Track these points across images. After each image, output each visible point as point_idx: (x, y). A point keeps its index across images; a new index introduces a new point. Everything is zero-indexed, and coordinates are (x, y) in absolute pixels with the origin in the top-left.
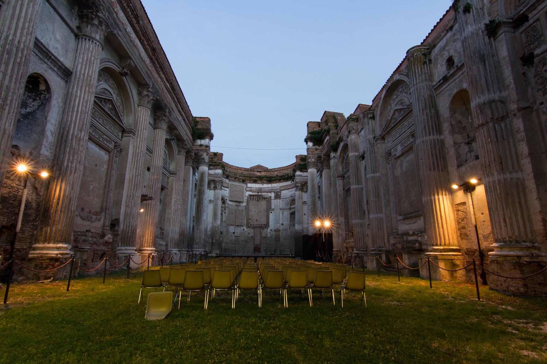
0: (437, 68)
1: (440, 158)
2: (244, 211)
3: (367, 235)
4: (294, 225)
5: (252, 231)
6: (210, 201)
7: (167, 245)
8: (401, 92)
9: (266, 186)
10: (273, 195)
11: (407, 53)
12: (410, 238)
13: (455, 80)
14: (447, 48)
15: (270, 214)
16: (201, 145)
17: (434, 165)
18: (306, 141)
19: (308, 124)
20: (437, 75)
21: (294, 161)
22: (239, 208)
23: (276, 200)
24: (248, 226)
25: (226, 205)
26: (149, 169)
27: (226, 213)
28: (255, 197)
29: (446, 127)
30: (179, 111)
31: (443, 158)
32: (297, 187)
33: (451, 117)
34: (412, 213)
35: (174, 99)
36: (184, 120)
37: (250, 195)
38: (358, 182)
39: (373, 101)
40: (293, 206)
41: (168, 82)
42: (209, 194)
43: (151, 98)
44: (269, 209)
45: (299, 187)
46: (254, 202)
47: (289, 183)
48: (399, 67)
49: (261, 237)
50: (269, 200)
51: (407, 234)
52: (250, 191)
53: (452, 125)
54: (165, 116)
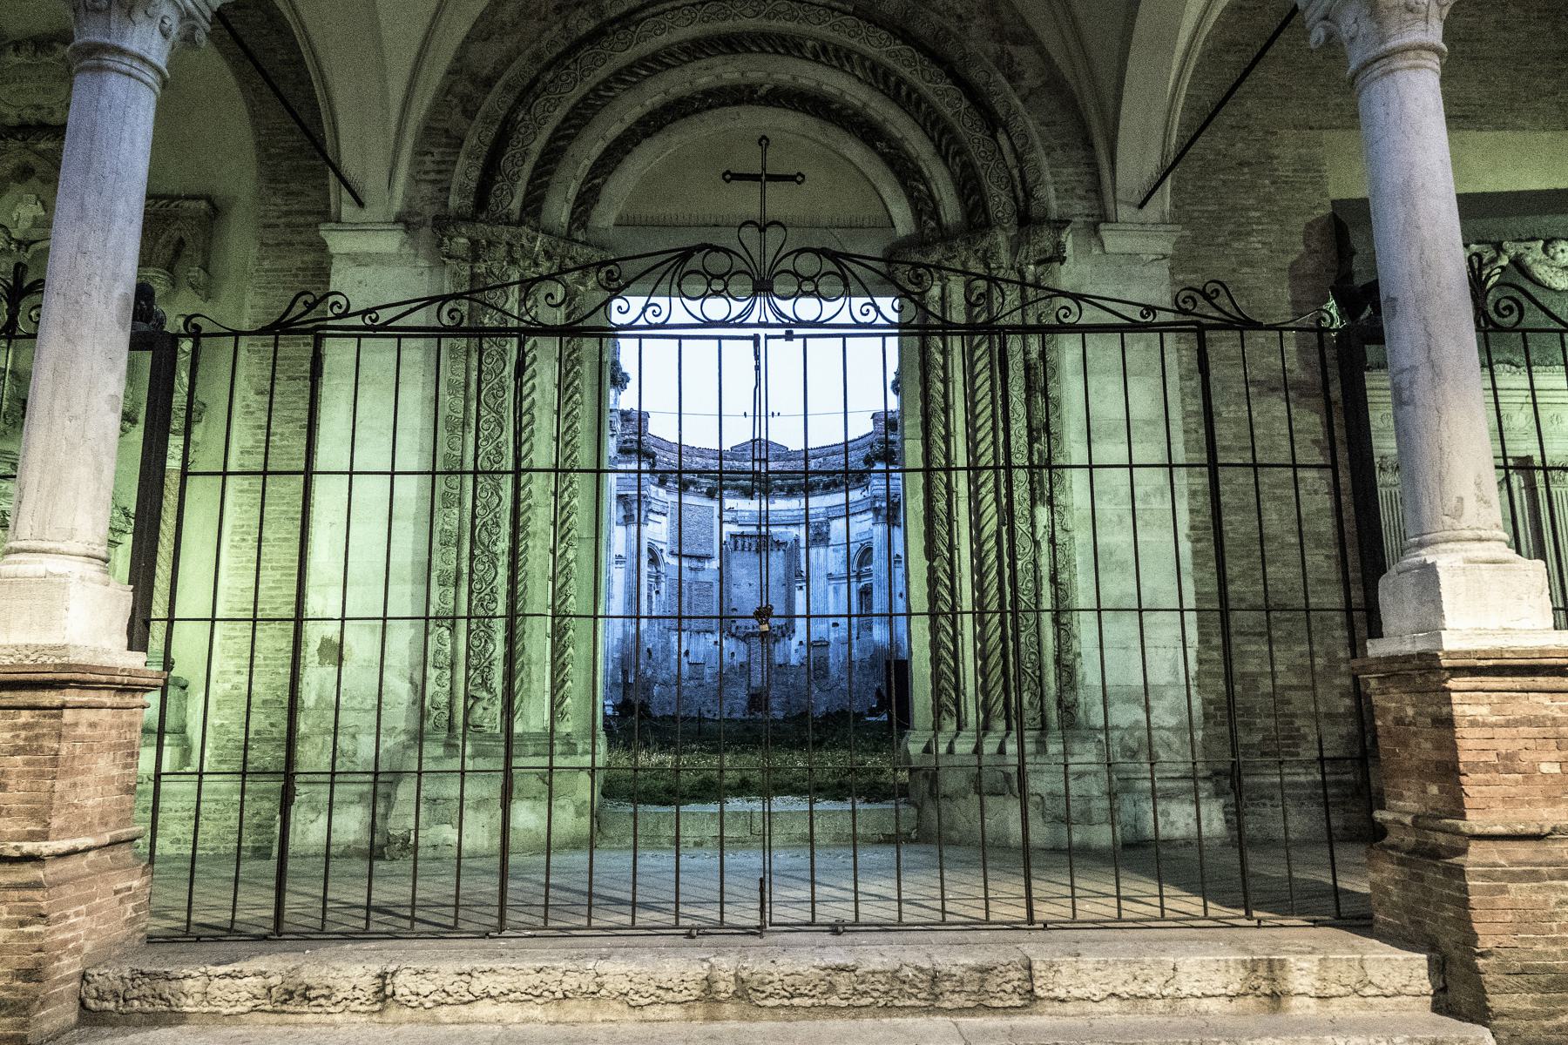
4: (871, 629)
5: (742, 644)
22: (702, 577)
25: (662, 569)
27: (663, 592)
32: (877, 511)
37: (733, 536)
45: (884, 512)
49: (770, 666)
50: (791, 550)
52: (734, 521)
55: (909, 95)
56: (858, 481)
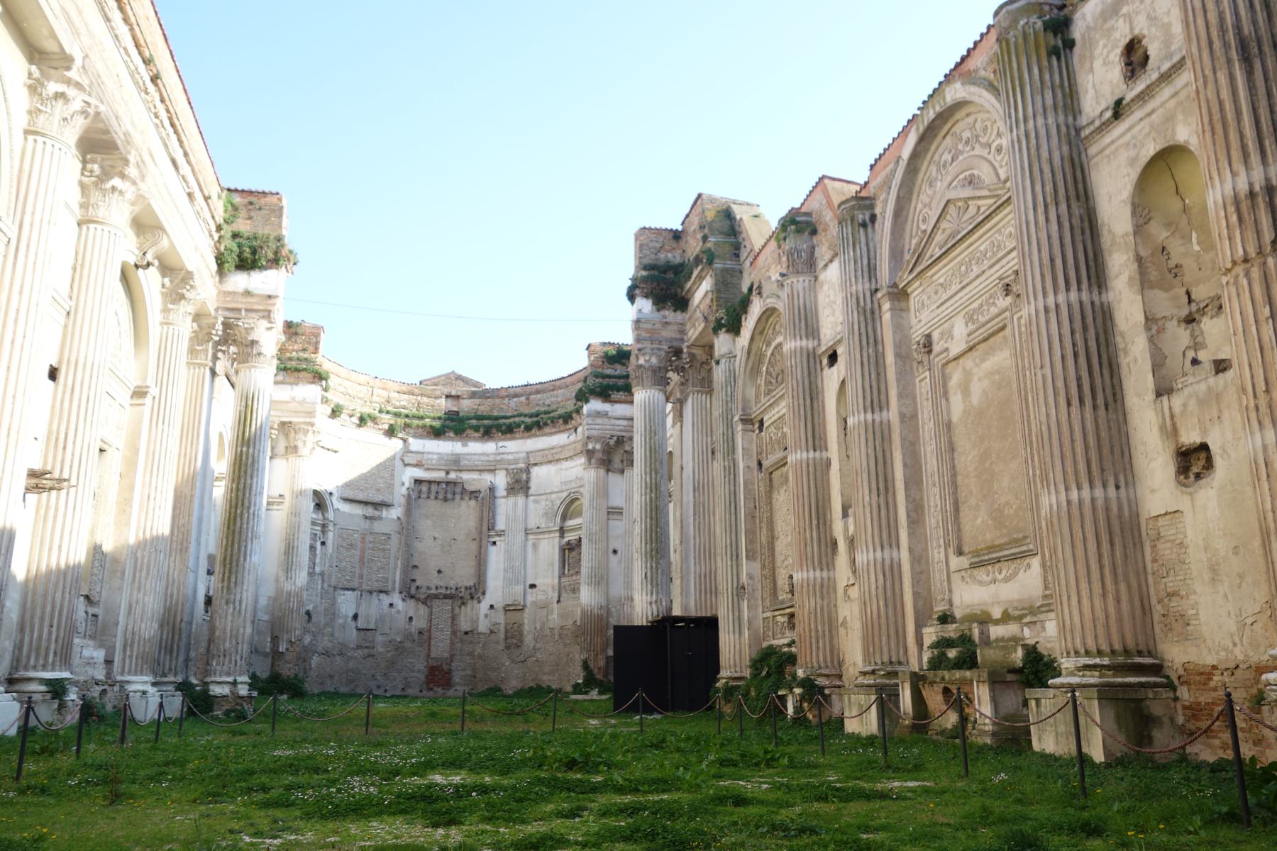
0: (1091, 70)
1: (1101, 364)
2: (395, 540)
3: (844, 623)
4: (575, 590)
5: (423, 610)
7: (109, 662)
8: (967, 143)
9: (477, 448)
10: (501, 480)
11: (996, 14)
12: (996, 632)
13: (1149, 115)
14: (1125, 10)
15: (492, 549)
16: (247, 293)
17: (1080, 386)
18: (631, 297)
20: (1091, 93)
21: (578, 361)
22: (378, 527)
23: (511, 500)
24: (409, 592)
26: (53, 374)
27: (329, 543)
28: (434, 487)
29: (1120, 265)
30: (174, 162)
31: (1110, 365)
32: (590, 454)
33: (1135, 234)
34: (1001, 547)
35: (157, 116)
36: (190, 195)
37: (418, 482)
38: (816, 440)
39: (872, 167)
40: (570, 523)
41: (140, 53)
43: (77, 105)
44: (487, 531)
45: (599, 455)
46: (432, 506)
47: (560, 439)
48: (963, 59)
49: (454, 633)
50: (487, 500)
51: (984, 620)
53: (1139, 260)
54: (123, 176)
56: (566, 422)
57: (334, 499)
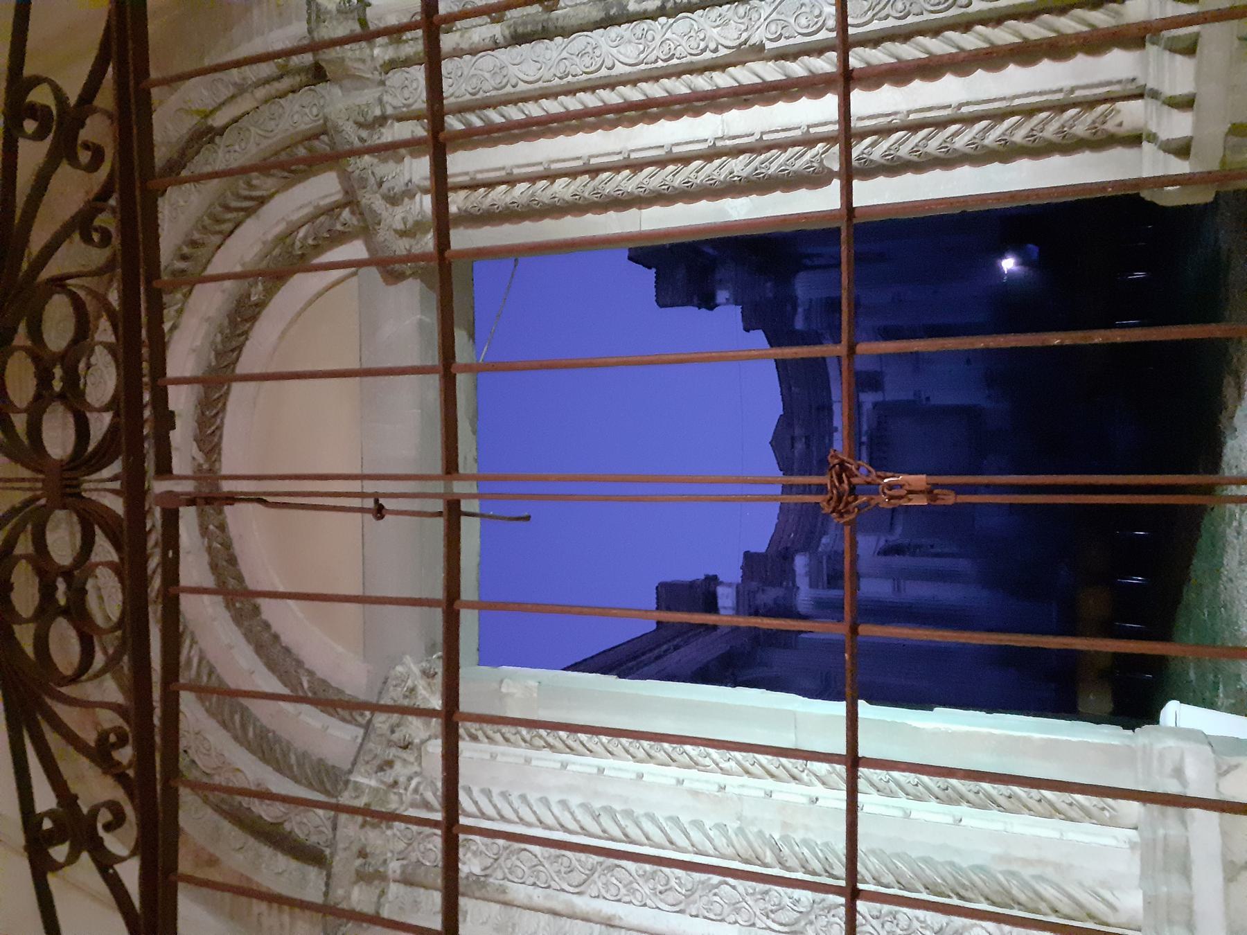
6: (898, 589)
9: (840, 418)
10: (868, 399)
15: (934, 401)
19: (661, 306)
42: (876, 588)
50: (885, 411)
55: (184, 258)
57: (891, 538)
